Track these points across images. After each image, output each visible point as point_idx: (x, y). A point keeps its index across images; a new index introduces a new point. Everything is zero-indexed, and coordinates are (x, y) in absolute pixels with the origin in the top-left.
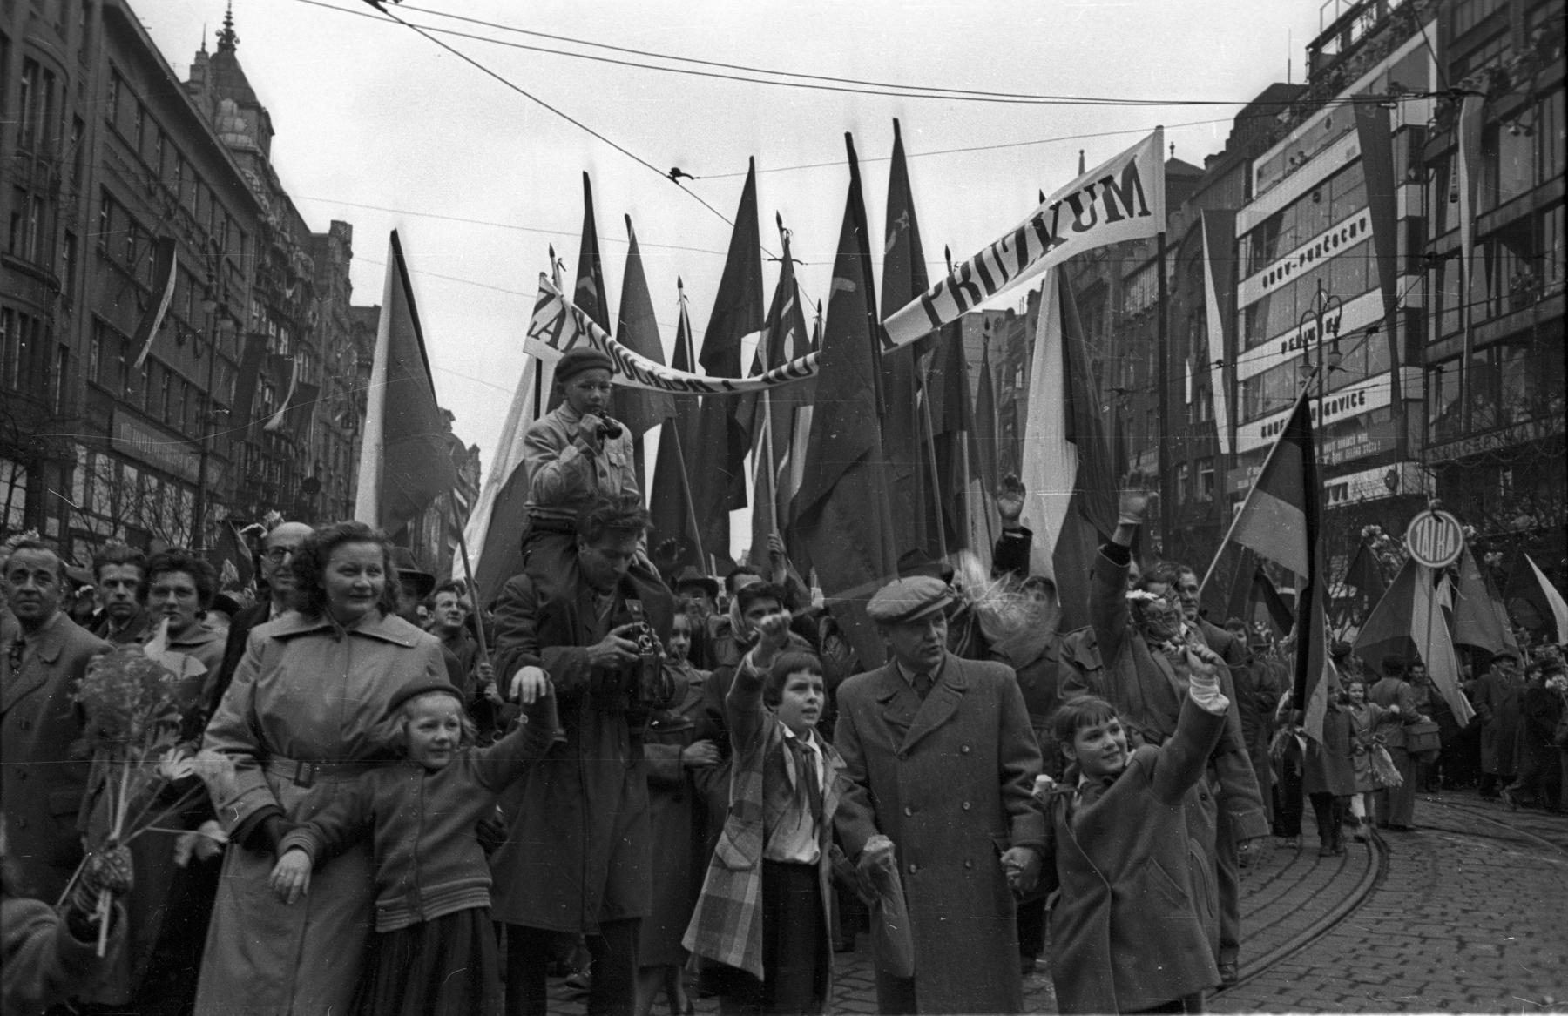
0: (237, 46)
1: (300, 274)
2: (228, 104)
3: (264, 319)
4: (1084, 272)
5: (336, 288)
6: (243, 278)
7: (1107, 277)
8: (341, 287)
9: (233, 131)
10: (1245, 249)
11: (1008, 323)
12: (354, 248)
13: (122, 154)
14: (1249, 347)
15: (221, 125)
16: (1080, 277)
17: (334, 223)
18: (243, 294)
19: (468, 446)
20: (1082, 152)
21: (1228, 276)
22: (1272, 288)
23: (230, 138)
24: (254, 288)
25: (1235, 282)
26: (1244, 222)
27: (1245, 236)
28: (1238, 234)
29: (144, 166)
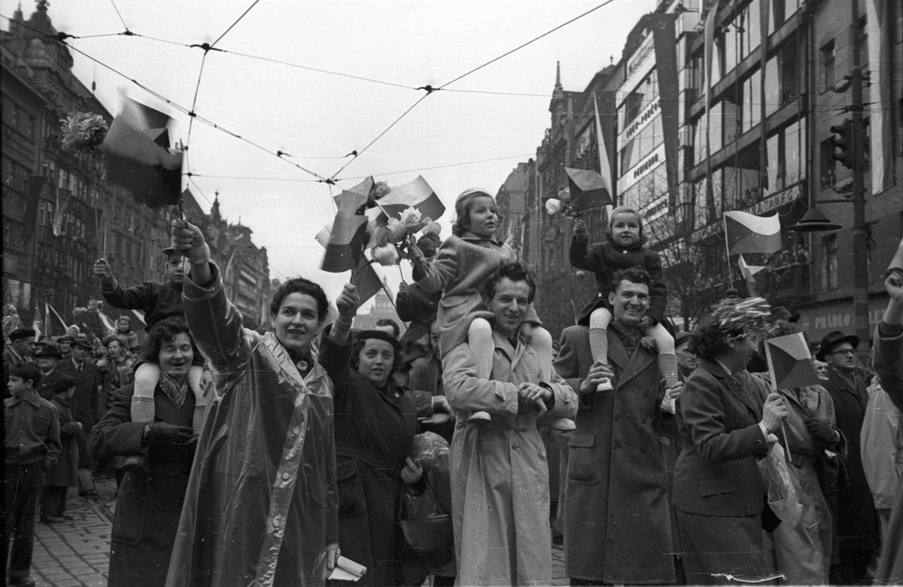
0: (48, 8)
2: (36, 41)
3: (53, 168)
4: (558, 134)
6: (33, 143)
7: (566, 137)
9: (38, 57)
10: (621, 114)
11: (529, 168)
14: (622, 175)
15: (30, 54)
18: (34, 154)
19: (259, 247)
20: (558, 62)
21: (612, 132)
22: (631, 138)
23: (35, 61)
24: (44, 149)
26: (620, 97)
27: (621, 106)
28: (617, 104)
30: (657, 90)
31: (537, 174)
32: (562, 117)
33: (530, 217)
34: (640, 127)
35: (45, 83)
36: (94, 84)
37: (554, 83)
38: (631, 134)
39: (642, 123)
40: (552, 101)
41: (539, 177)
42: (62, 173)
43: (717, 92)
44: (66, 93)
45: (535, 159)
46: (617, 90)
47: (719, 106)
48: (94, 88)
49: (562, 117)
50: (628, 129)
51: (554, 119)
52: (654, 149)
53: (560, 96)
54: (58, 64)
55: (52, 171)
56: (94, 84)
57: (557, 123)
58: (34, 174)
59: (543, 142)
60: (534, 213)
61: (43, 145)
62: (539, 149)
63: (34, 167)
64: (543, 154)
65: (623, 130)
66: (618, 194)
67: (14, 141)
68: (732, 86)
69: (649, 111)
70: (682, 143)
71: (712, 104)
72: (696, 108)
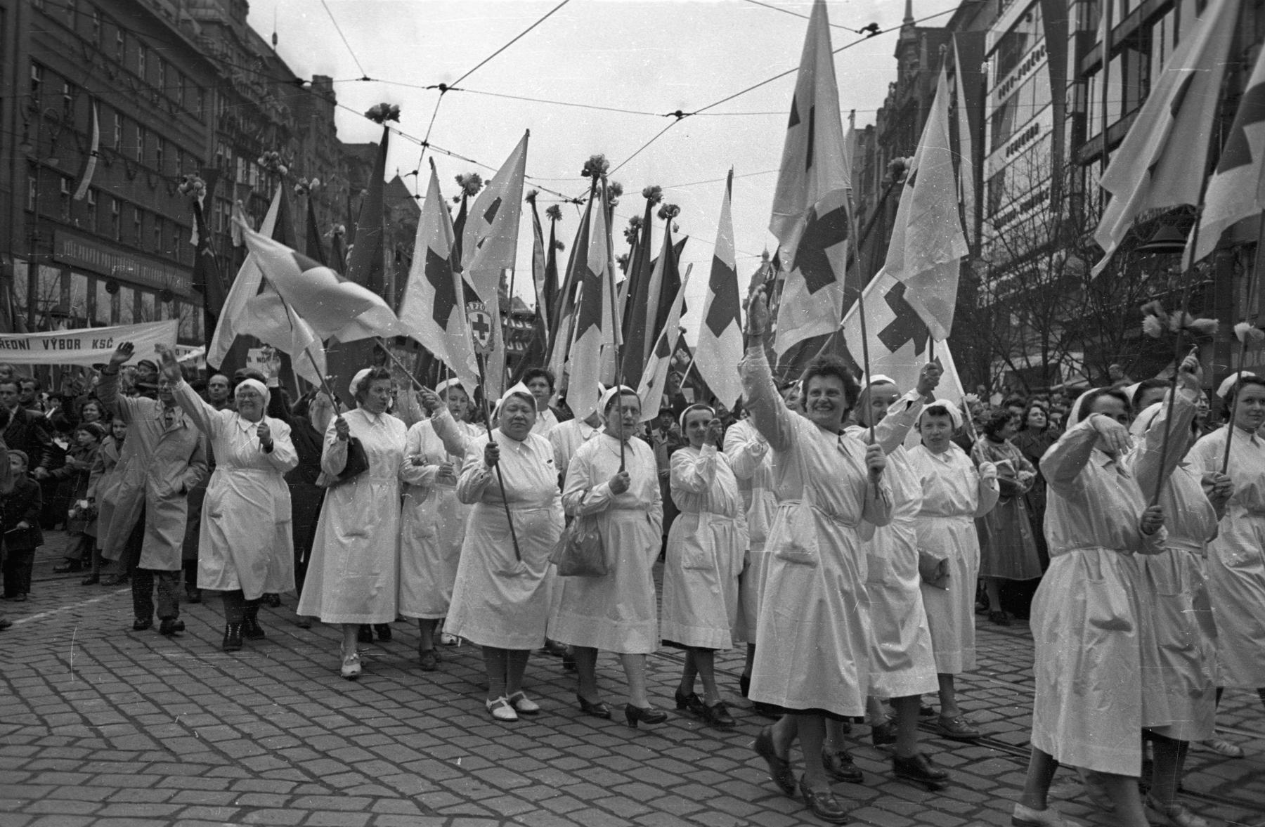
1: (275, 119)
3: (229, 157)
5: (317, 129)
6: (204, 125)
7: (917, 94)
8: (326, 130)
11: (868, 137)
12: (338, 99)
13: (53, 30)
16: (904, 96)
17: (315, 77)
18: (204, 138)
22: (1004, 99)
23: (202, 12)
24: (217, 132)
25: (984, 94)
26: (990, 41)
27: (992, 52)
29: (79, 38)
30: (1041, 31)
31: (877, 147)
32: (913, 66)
33: (865, 209)
34: (1018, 84)
35: (217, 44)
36: (275, 36)
37: (903, 16)
38: (1004, 94)
39: (1019, 78)
40: (899, 43)
41: (879, 153)
42: (240, 160)
43: (1118, 38)
44: (242, 54)
45: (874, 124)
46: (987, 30)
47: (1118, 60)
48: (275, 42)
49: (913, 66)
50: (1000, 86)
51: (901, 68)
52: (1034, 116)
53: (911, 36)
54: (231, 14)
55: (228, 160)
56: (275, 36)
57: (906, 76)
58: (206, 166)
59: (886, 101)
60: (871, 203)
61: (216, 127)
62: (880, 111)
63: (206, 156)
64: (885, 120)
65: (995, 87)
66: (985, 178)
67: (181, 122)
68: (1134, 33)
69: (1028, 62)
70: (1070, 109)
71: (1111, 57)
72: (1091, 59)
